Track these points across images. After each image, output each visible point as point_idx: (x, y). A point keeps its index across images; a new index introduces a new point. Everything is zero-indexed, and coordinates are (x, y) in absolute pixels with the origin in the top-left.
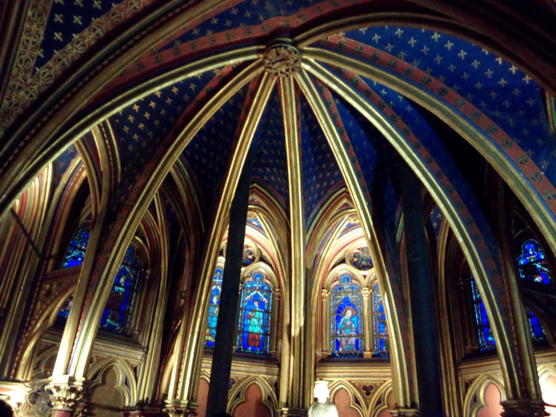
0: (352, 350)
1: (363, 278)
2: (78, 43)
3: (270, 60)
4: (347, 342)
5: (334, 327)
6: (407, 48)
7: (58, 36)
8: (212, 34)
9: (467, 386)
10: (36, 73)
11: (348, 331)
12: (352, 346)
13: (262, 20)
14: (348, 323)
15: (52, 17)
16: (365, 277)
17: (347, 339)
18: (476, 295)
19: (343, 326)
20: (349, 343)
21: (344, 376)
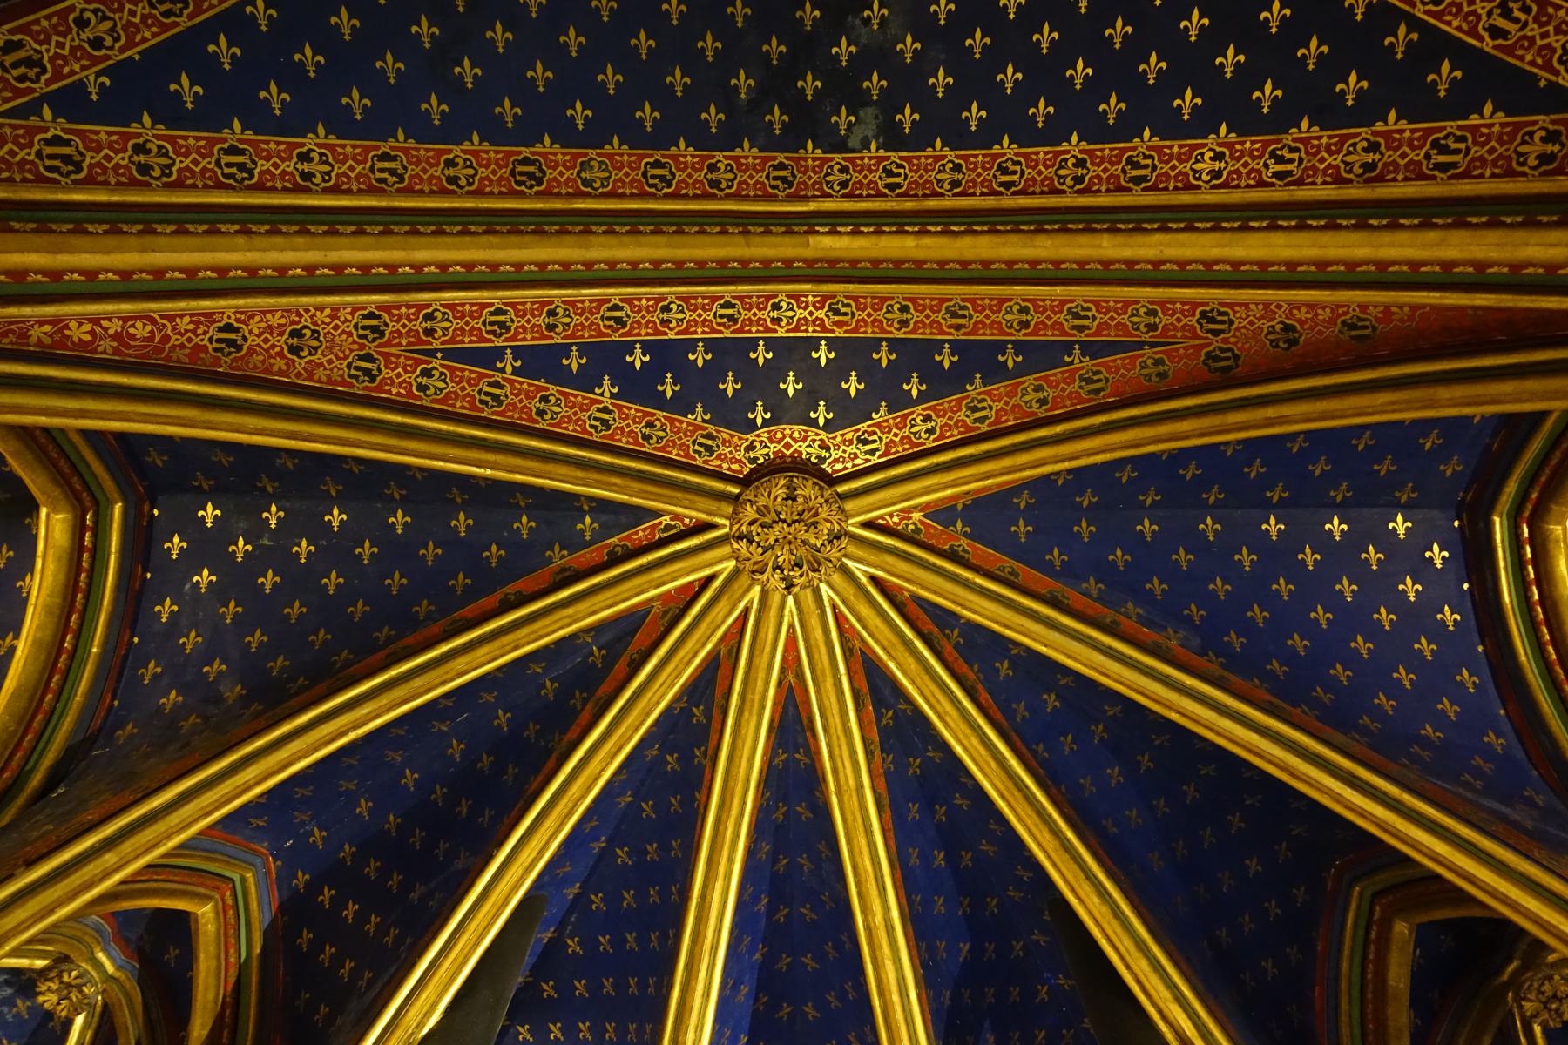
2: (233, 151)
3: (758, 511)
6: (1145, 598)
7: (187, 88)
8: (613, 396)
10: (34, 121)
13: (759, 422)
15: (207, 31)
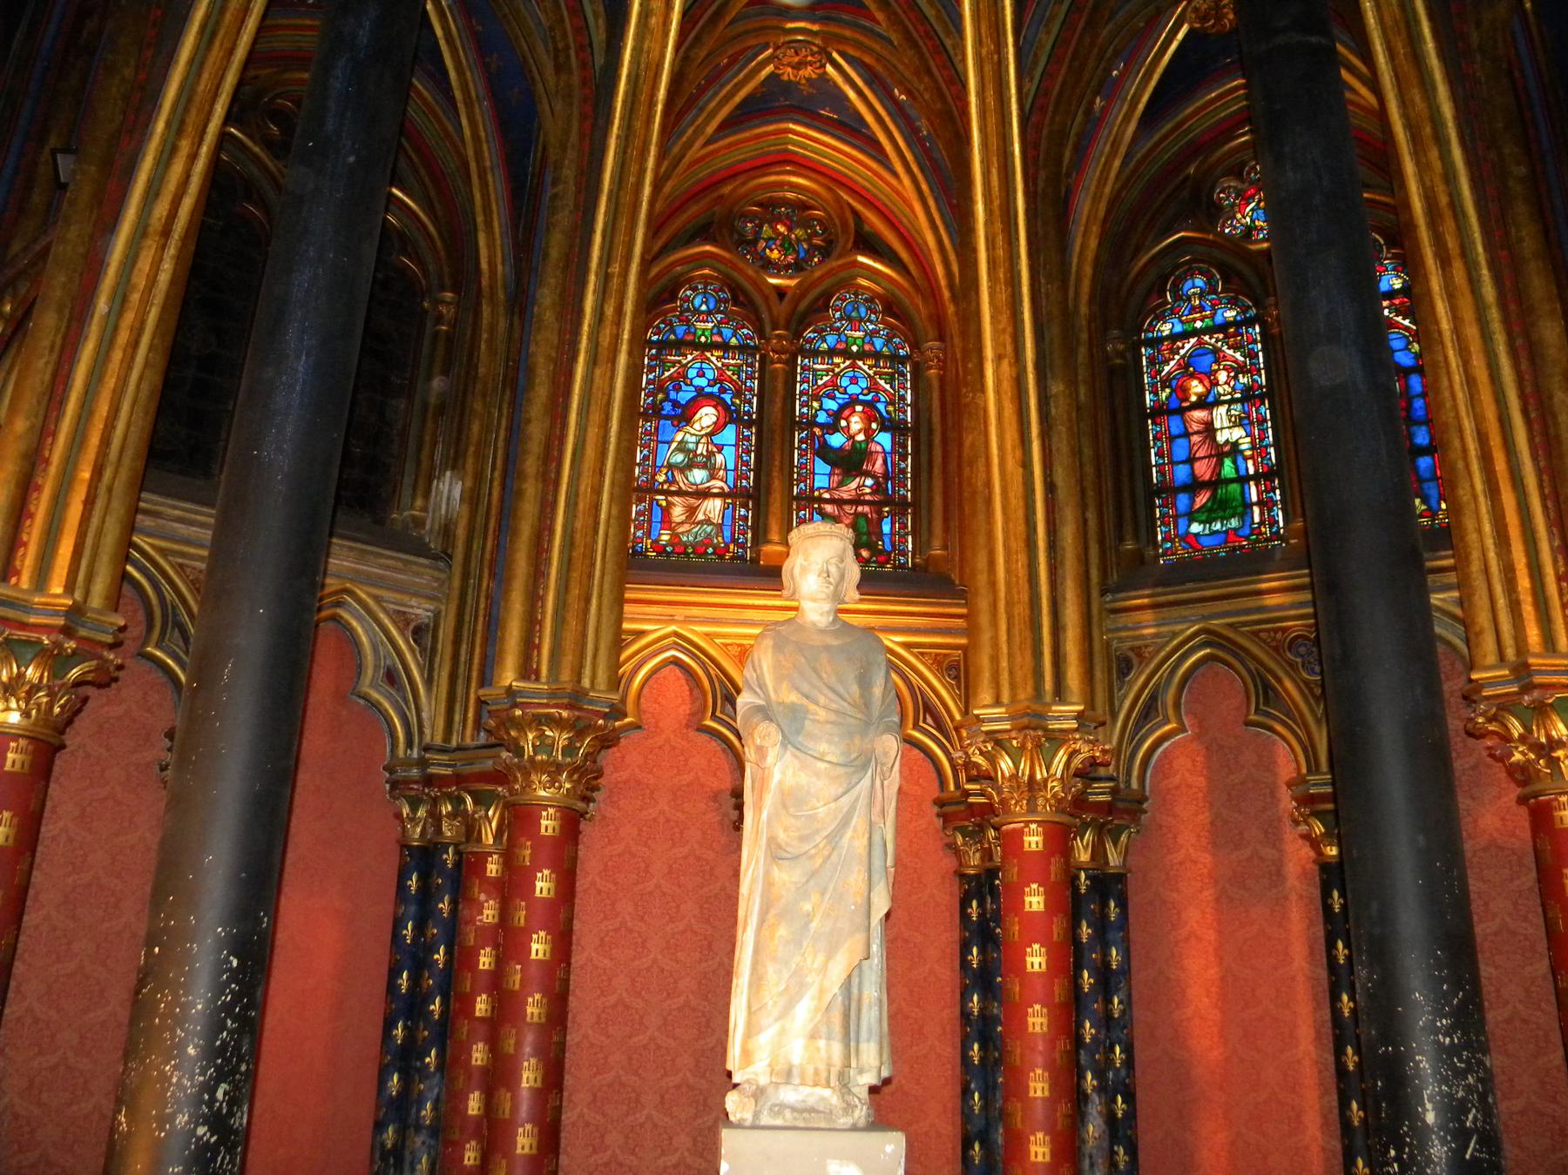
0: (708, 541)
1: (774, 297)
4: (691, 511)
5: (645, 458)
9: (1123, 666)
11: (698, 475)
12: (709, 529)
14: (701, 449)
16: (781, 292)
17: (692, 501)
18: (1155, 393)
19: (679, 458)
20: (701, 517)
21: (689, 620)
